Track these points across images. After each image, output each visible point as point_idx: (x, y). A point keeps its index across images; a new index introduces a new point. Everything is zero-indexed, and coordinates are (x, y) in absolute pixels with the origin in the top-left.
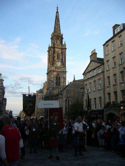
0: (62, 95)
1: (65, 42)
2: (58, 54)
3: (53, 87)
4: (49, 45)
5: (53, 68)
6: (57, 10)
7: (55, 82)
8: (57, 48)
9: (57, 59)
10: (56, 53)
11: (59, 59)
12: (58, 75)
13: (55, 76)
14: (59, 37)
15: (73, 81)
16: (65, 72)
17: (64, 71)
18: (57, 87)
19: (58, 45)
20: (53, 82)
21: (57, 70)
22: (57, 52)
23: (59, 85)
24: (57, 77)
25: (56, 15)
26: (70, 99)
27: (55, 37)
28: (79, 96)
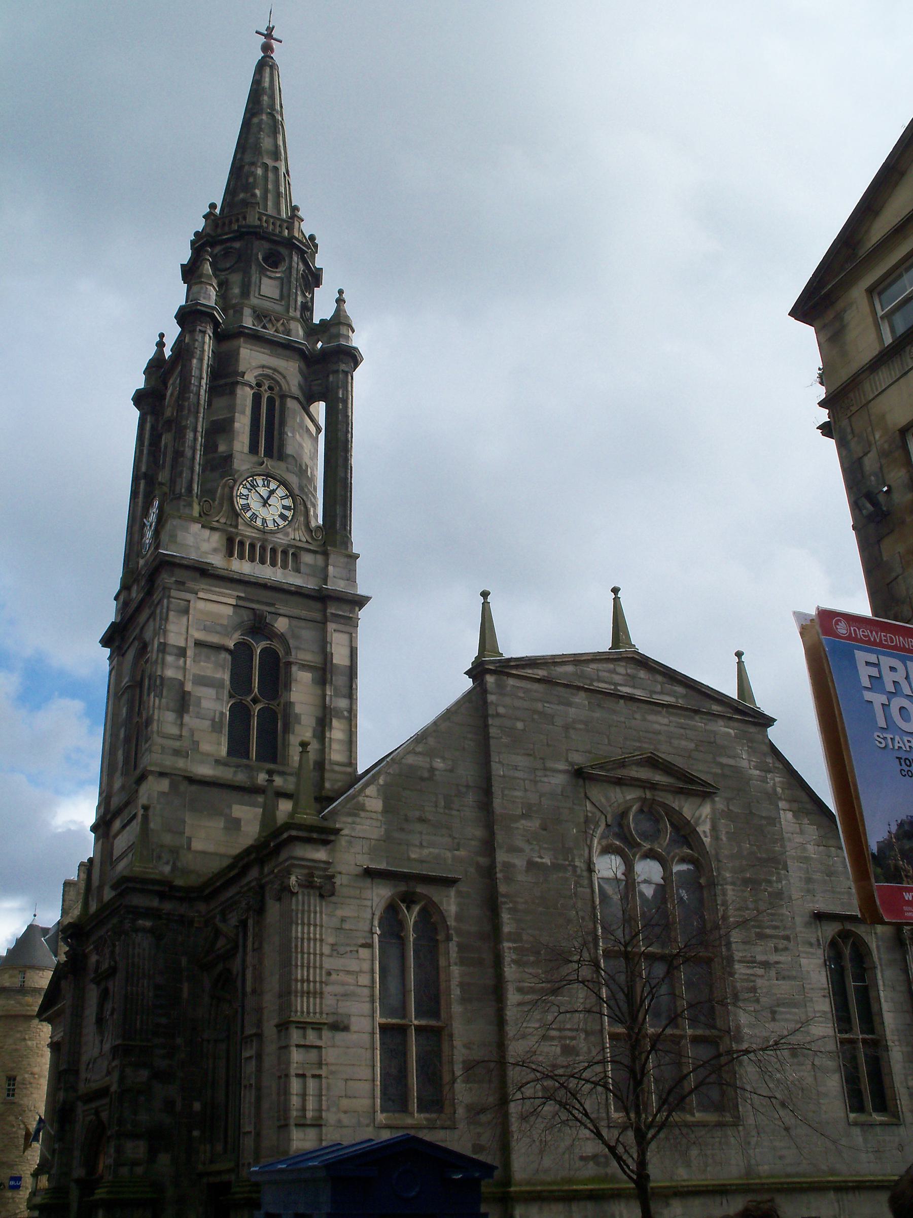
0: (325, 835)
1: (340, 301)
2: (257, 398)
3: (181, 763)
4: (161, 345)
5: (199, 542)
6: (267, 48)
7: (213, 703)
8: (256, 338)
9: (254, 448)
10: (245, 395)
11: (269, 453)
12: (258, 627)
13: (214, 639)
14: (283, 251)
15: (477, 672)
16: (338, 606)
17: (336, 584)
18: (241, 778)
19: (260, 316)
20: (183, 703)
21: (243, 567)
22: (250, 377)
23: (272, 750)
24: (240, 656)
25: (257, 83)
26: (450, 904)
27: (237, 245)
28: (556, 867)
